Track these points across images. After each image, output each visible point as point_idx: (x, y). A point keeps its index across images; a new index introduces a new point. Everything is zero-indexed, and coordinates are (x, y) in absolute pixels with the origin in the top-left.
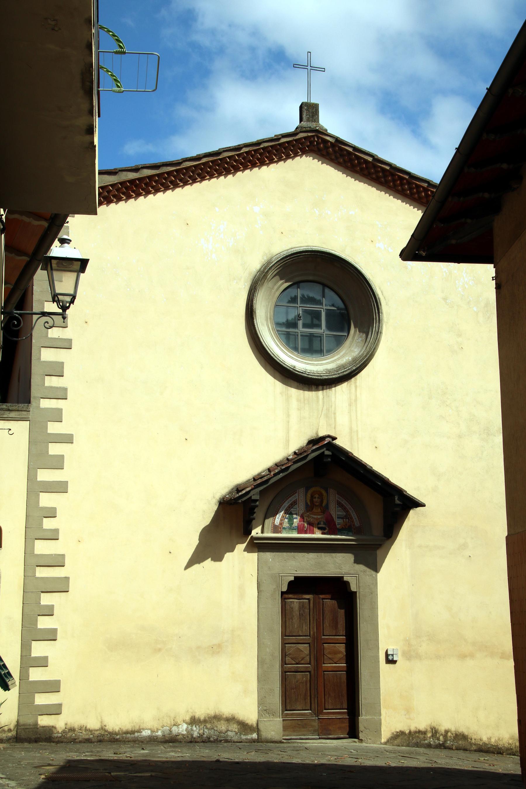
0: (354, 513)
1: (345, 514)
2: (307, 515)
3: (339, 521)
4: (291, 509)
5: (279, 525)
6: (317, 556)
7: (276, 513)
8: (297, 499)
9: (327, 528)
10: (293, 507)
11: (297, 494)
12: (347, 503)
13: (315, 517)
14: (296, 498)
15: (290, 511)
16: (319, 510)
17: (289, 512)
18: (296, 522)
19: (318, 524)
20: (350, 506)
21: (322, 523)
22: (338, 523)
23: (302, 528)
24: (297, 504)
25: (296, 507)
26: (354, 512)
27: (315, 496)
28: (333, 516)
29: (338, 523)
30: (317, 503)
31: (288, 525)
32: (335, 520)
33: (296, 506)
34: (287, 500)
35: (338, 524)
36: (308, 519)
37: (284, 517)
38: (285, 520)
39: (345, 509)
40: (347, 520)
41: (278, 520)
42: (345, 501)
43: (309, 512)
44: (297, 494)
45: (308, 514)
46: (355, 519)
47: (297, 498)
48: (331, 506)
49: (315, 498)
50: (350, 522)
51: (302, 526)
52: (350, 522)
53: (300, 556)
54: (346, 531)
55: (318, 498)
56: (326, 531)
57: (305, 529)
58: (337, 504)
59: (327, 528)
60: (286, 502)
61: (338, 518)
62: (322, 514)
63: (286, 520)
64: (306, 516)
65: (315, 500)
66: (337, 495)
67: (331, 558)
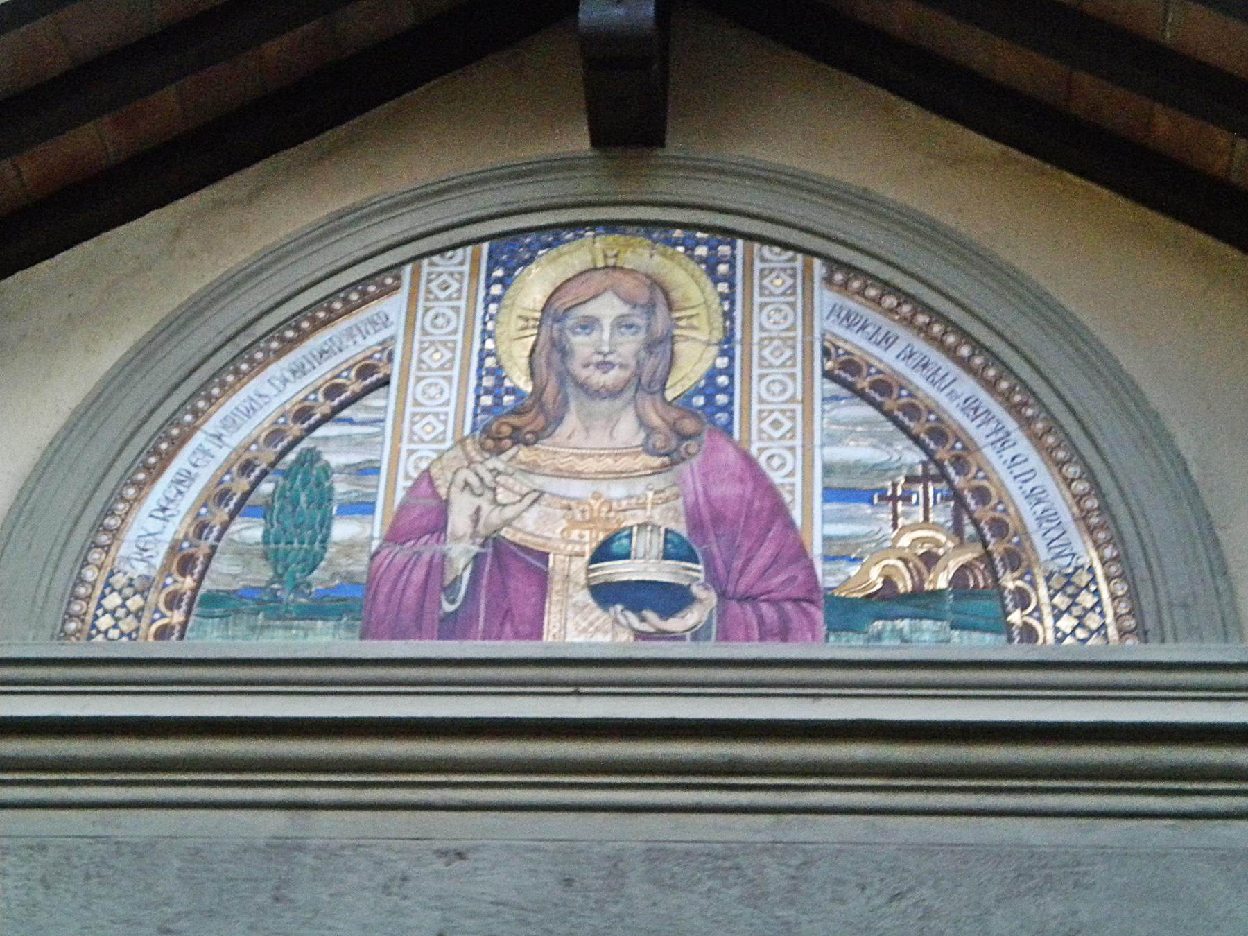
0: (1023, 446)
1: (914, 457)
2: (488, 478)
3: (833, 530)
4: (320, 432)
5: (165, 570)
6: (568, 882)
7: (147, 468)
8: (392, 338)
9: (708, 598)
10: (345, 413)
11: (402, 295)
12: (936, 357)
13: (577, 489)
14: (384, 334)
15: (304, 444)
16: (627, 430)
17: (291, 457)
18: (349, 548)
19: (603, 553)
20: (968, 386)
21: (647, 544)
22: (827, 539)
23: (411, 595)
24: (385, 382)
25: (367, 408)
26: (1017, 435)
27: (590, 309)
28: (776, 478)
29: (827, 539)
30: (605, 366)
31: (262, 574)
32: (797, 515)
33: (373, 400)
34: (279, 354)
35: (827, 558)
36: (492, 517)
37: (223, 497)
38: (234, 528)
39: (912, 410)
40: (942, 515)
41: (154, 525)
42: (922, 347)
43: (511, 452)
44: (394, 306)
45: (496, 472)
46: (1035, 496)
47: (397, 327)
48: (759, 388)
49: (589, 324)
50: (970, 530)
51: (419, 575)
52: (970, 530)
53: (353, 879)
54: (927, 624)
55: (622, 324)
56: (691, 618)
57: (448, 607)
58: (827, 374)
59: (695, 590)
60: (278, 368)
61: (830, 494)
62: (657, 461)
63: (250, 531)
64: (467, 484)
65: (582, 345)
66: (825, 298)
67: (741, 900)
